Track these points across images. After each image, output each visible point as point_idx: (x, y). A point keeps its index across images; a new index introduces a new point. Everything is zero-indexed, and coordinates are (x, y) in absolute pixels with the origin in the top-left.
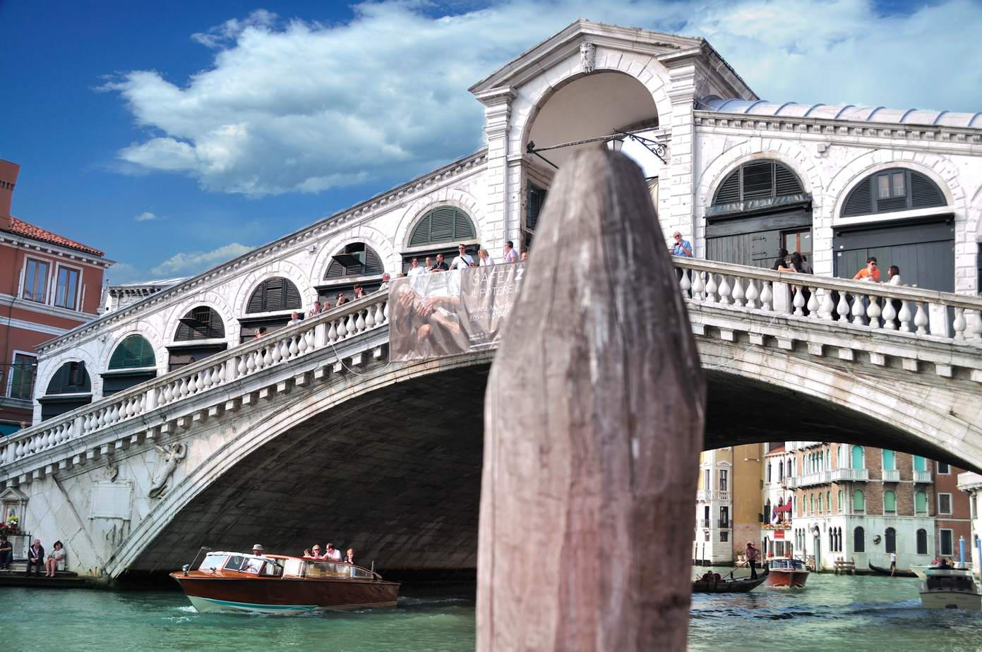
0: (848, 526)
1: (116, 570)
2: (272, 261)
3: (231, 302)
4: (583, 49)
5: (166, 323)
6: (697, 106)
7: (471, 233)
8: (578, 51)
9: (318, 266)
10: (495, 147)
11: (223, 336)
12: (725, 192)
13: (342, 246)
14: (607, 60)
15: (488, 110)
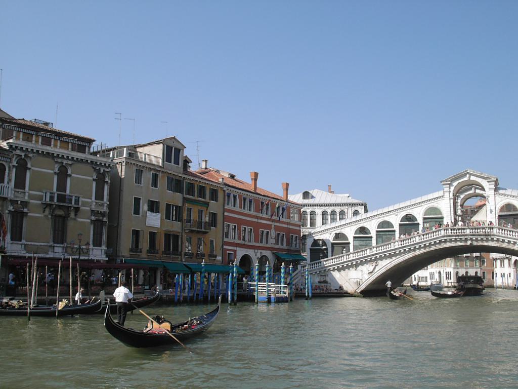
0: (454, 271)
1: (359, 291)
2: (384, 217)
3: (372, 226)
4: (468, 175)
5: (351, 230)
6: (495, 191)
7: (441, 214)
8: (466, 175)
9: (398, 218)
10: (447, 195)
11: (370, 234)
12: (502, 209)
13: (405, 214)
14: (473, 178)
15: (444, 186)
